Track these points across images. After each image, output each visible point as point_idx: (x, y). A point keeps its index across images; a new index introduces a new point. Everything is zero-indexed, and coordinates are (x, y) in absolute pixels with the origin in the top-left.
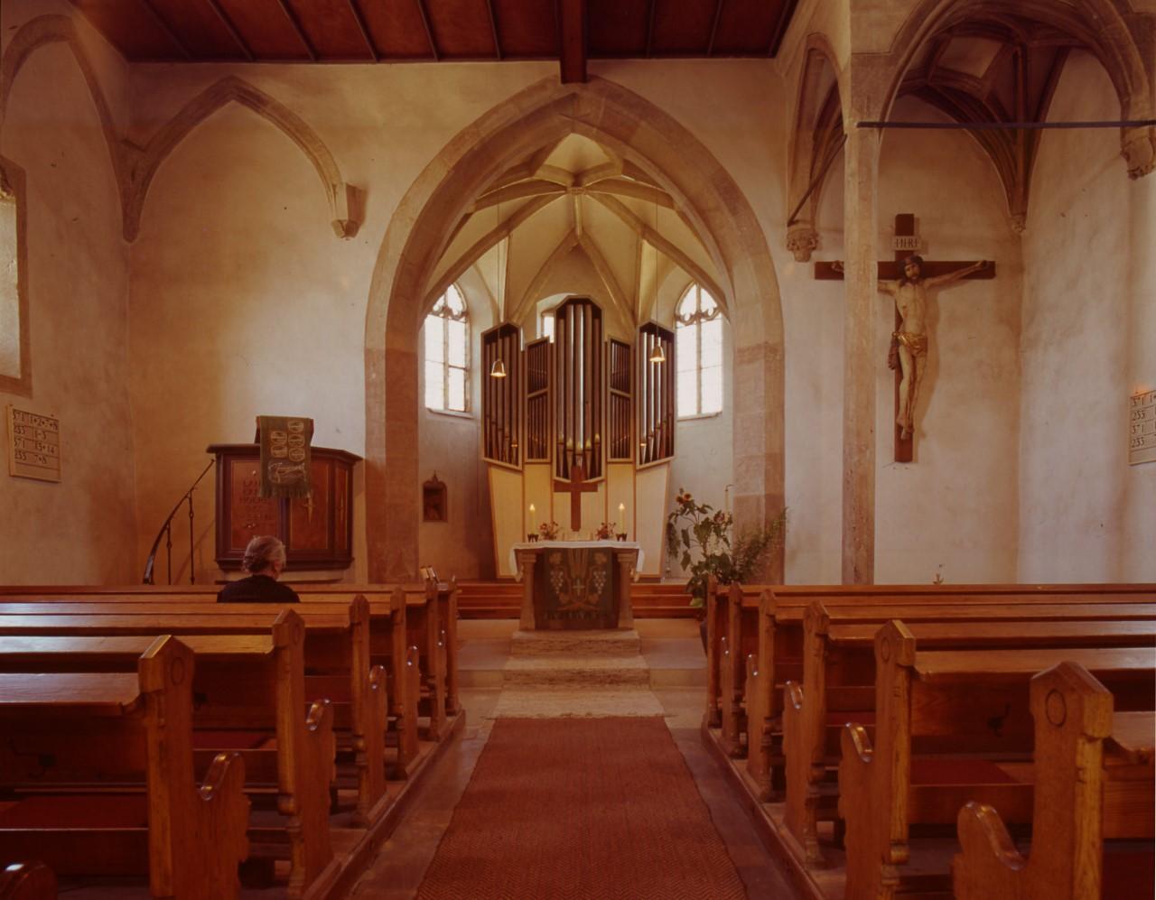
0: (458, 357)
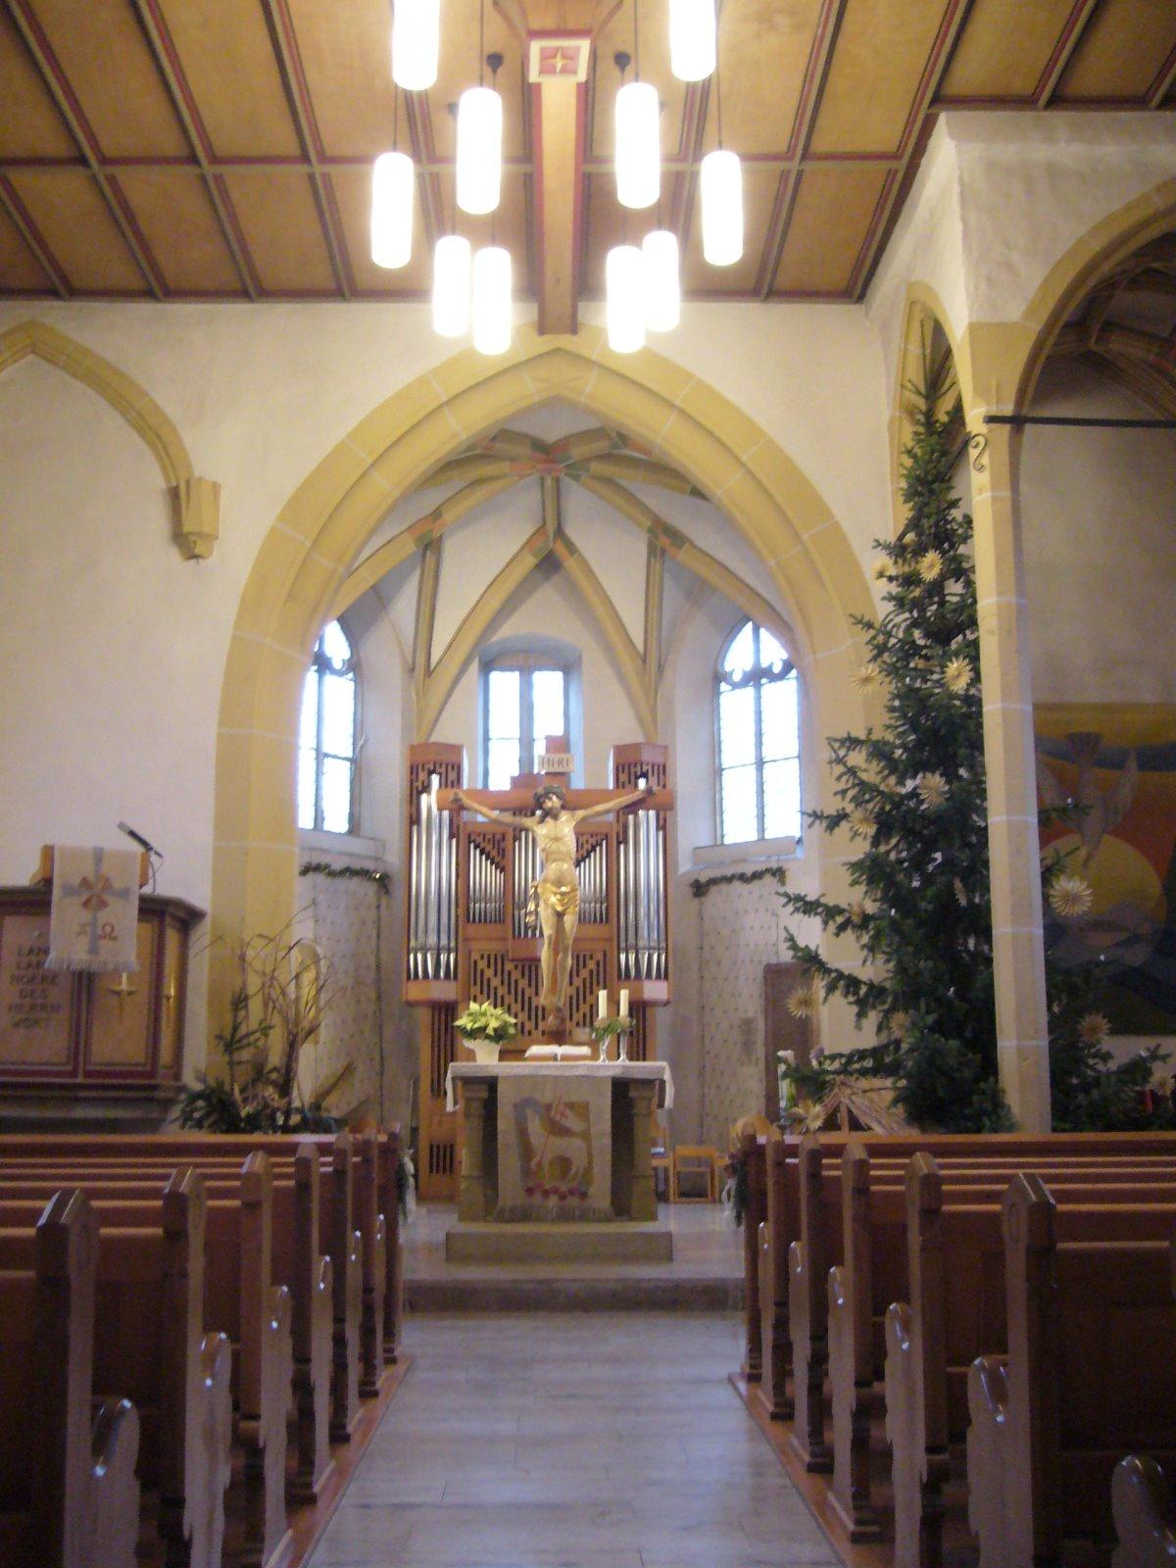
0: (339, 739)
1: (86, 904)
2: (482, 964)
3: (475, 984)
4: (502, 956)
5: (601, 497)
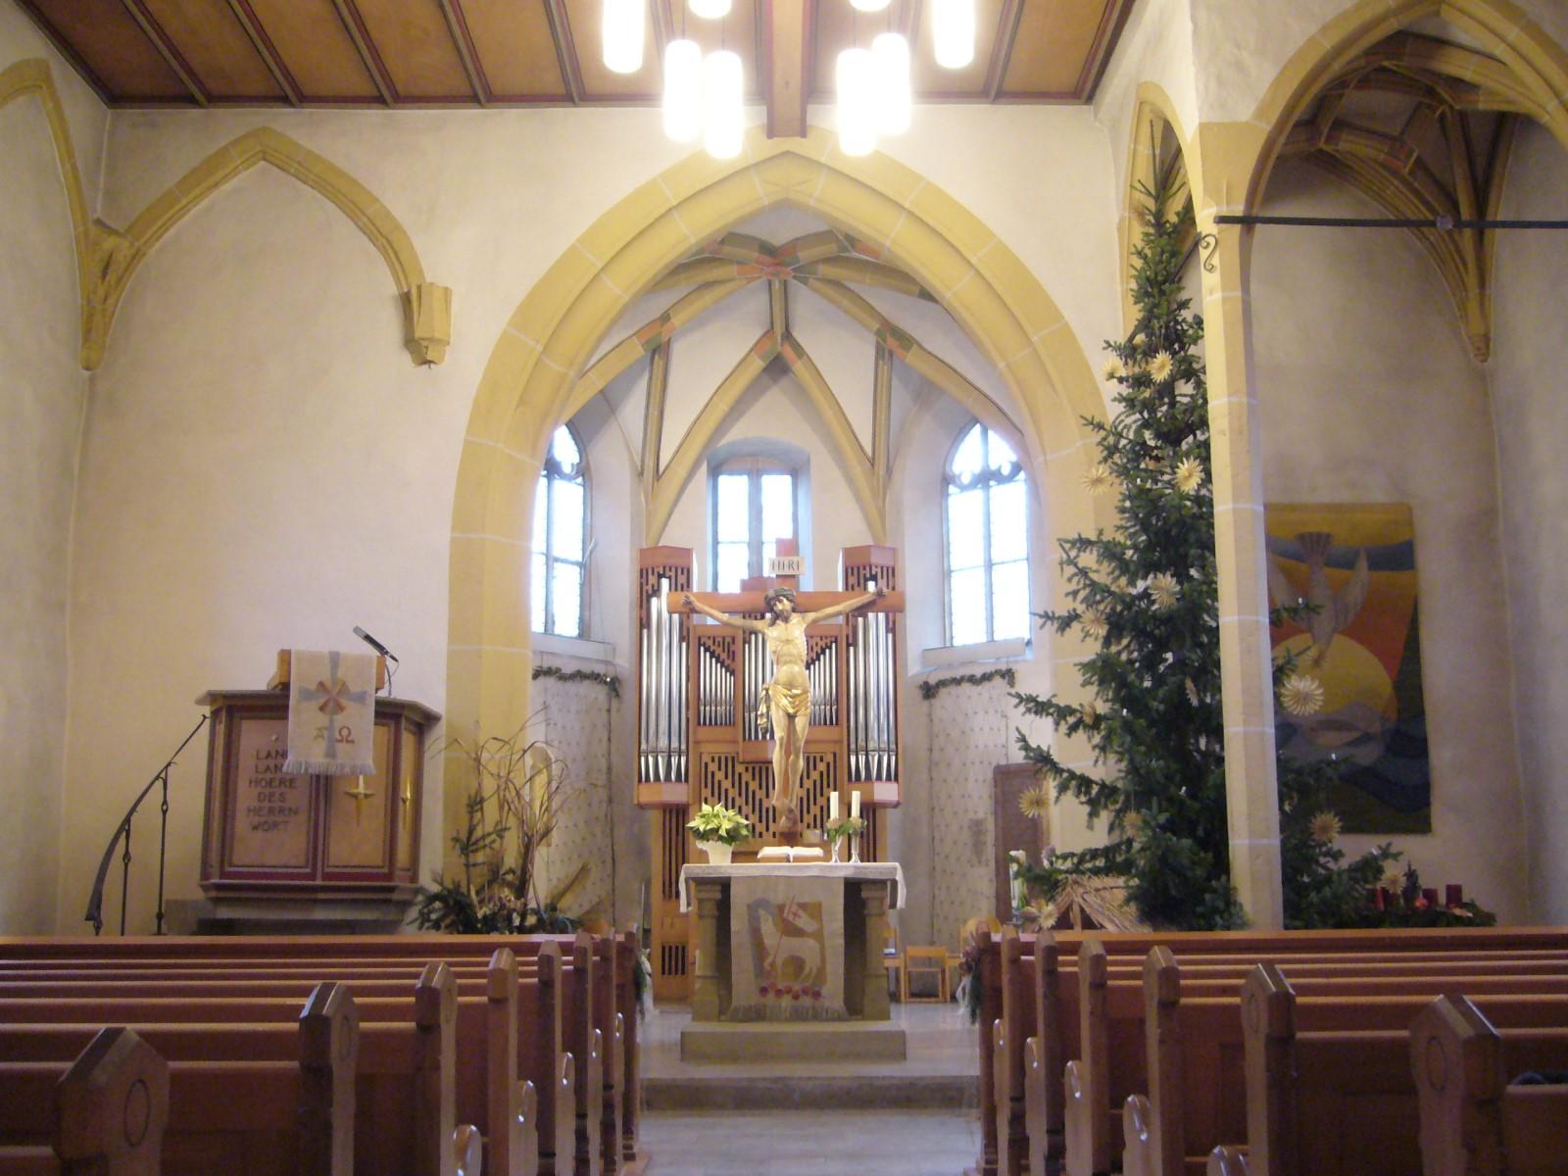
0: (569, 543)
1: (322, 709)
2: (713, 767)
3: (706, 786)
4: (733, 758)
5: (832, 301)
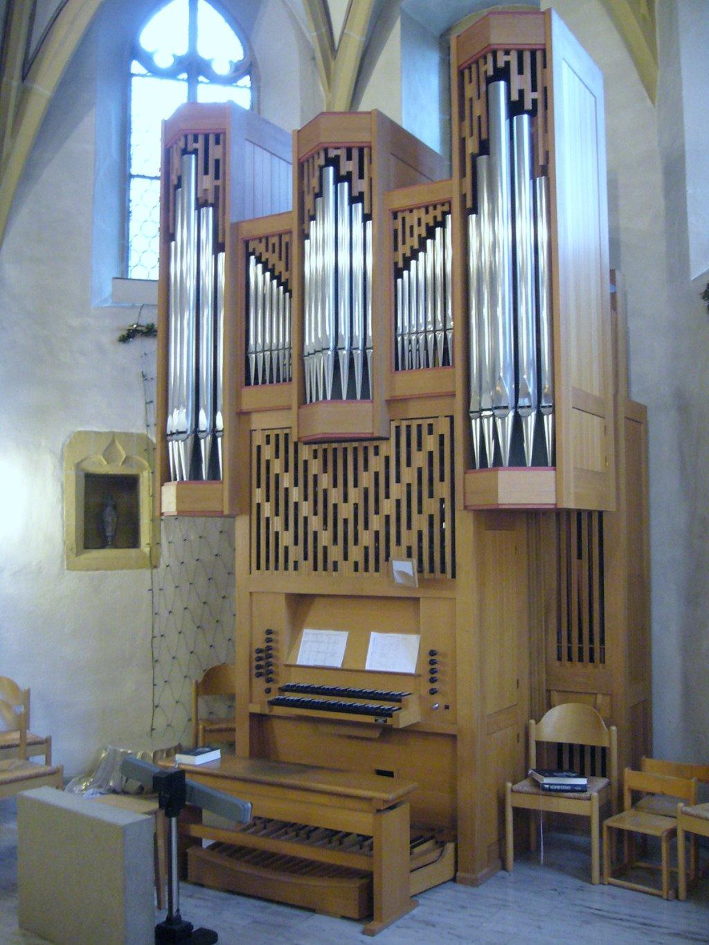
2: (268, 452)
